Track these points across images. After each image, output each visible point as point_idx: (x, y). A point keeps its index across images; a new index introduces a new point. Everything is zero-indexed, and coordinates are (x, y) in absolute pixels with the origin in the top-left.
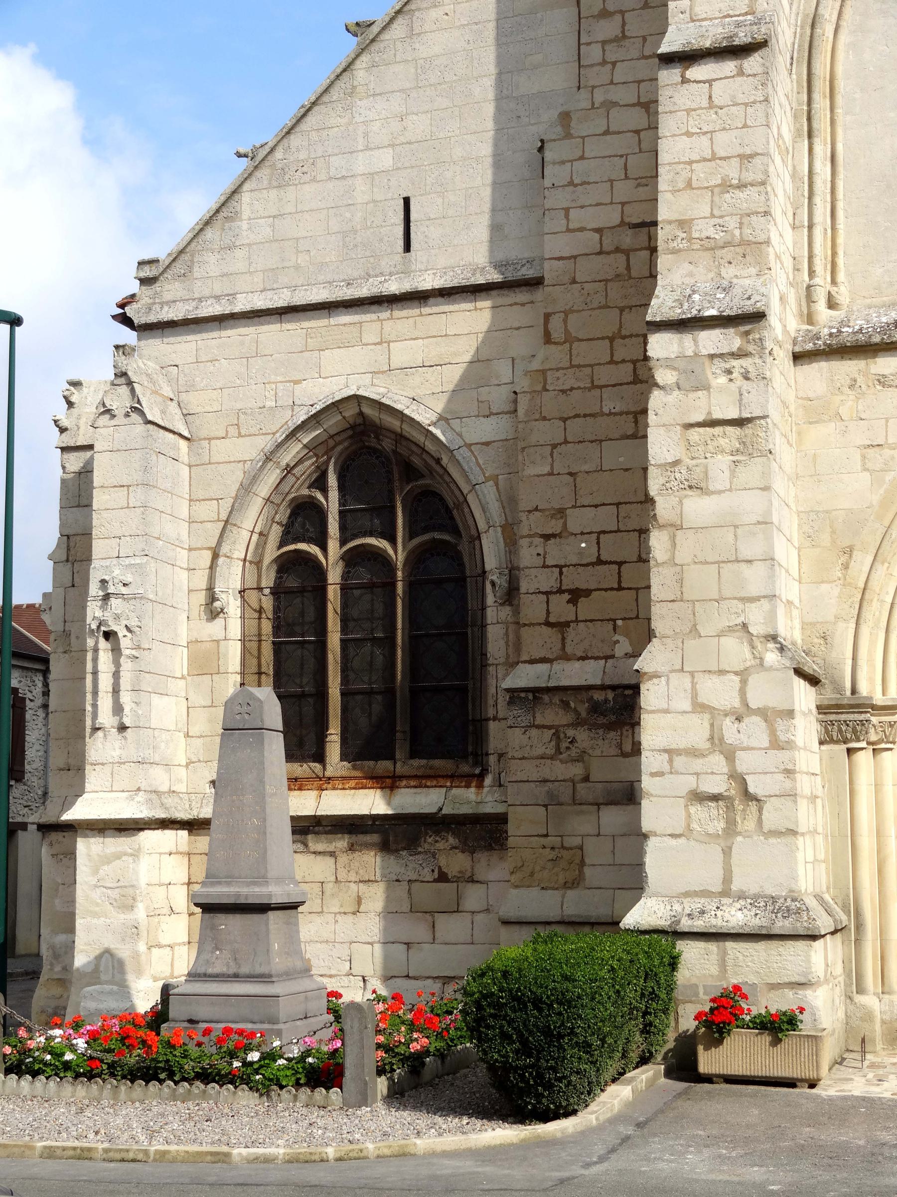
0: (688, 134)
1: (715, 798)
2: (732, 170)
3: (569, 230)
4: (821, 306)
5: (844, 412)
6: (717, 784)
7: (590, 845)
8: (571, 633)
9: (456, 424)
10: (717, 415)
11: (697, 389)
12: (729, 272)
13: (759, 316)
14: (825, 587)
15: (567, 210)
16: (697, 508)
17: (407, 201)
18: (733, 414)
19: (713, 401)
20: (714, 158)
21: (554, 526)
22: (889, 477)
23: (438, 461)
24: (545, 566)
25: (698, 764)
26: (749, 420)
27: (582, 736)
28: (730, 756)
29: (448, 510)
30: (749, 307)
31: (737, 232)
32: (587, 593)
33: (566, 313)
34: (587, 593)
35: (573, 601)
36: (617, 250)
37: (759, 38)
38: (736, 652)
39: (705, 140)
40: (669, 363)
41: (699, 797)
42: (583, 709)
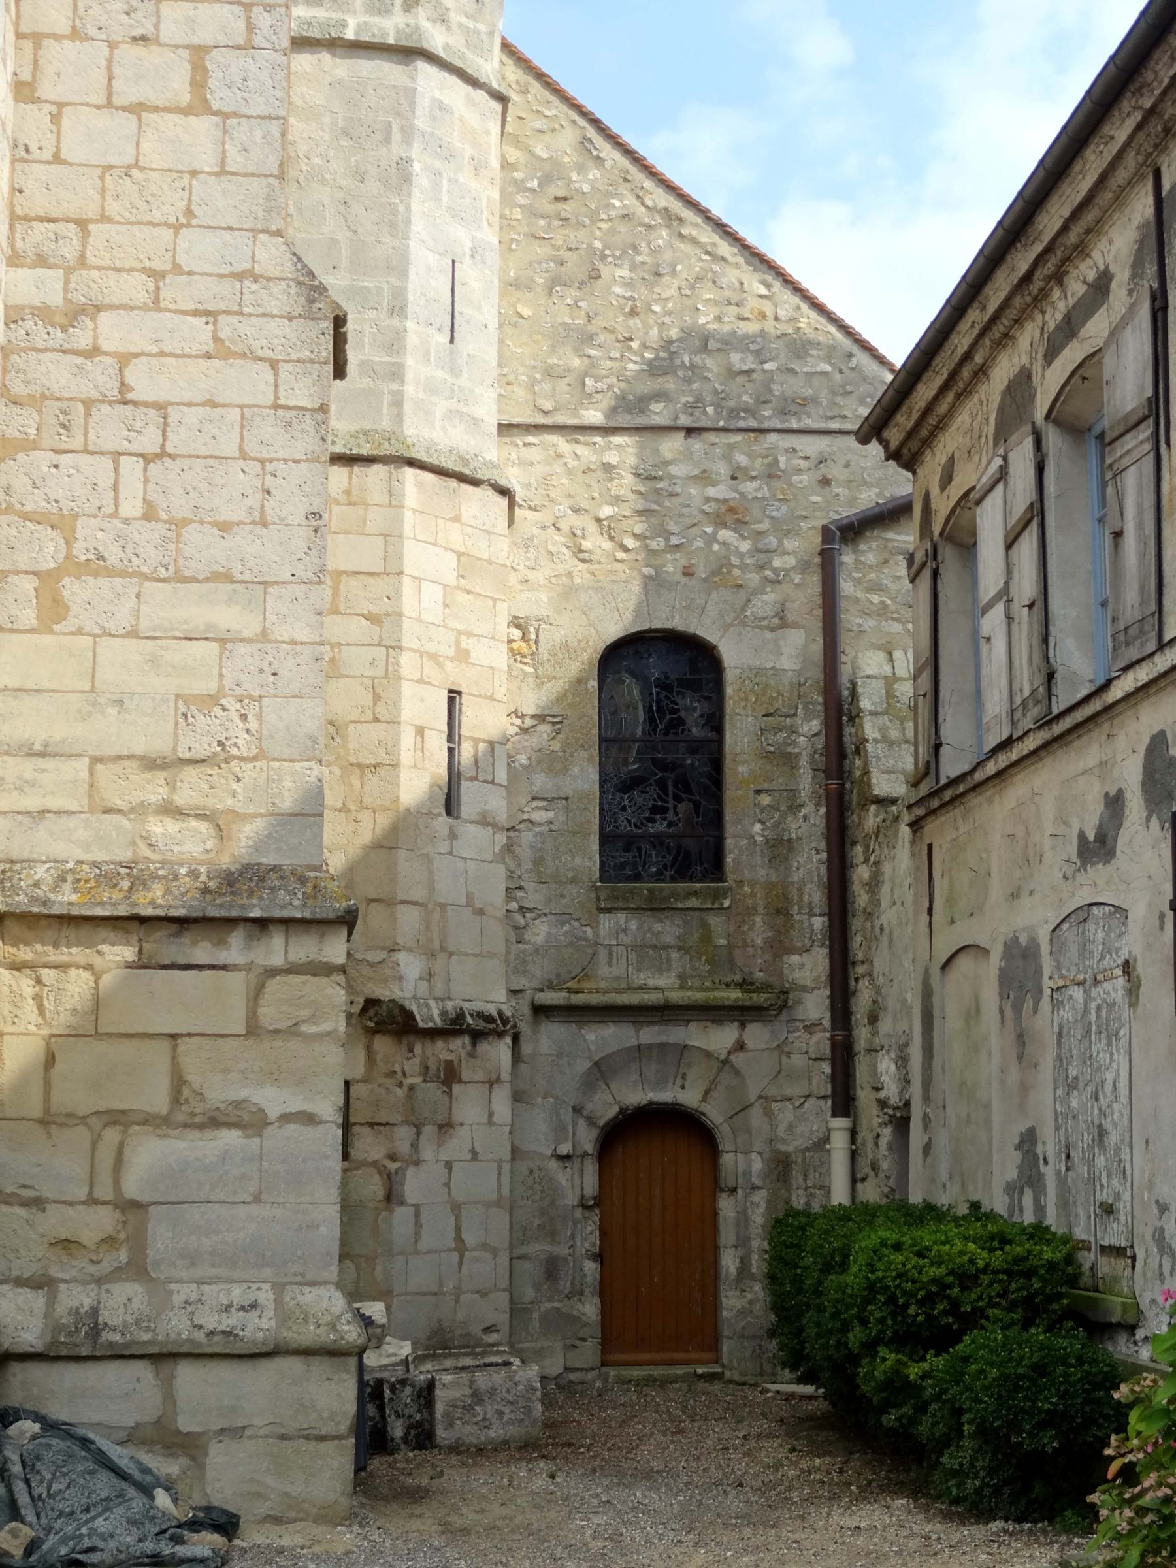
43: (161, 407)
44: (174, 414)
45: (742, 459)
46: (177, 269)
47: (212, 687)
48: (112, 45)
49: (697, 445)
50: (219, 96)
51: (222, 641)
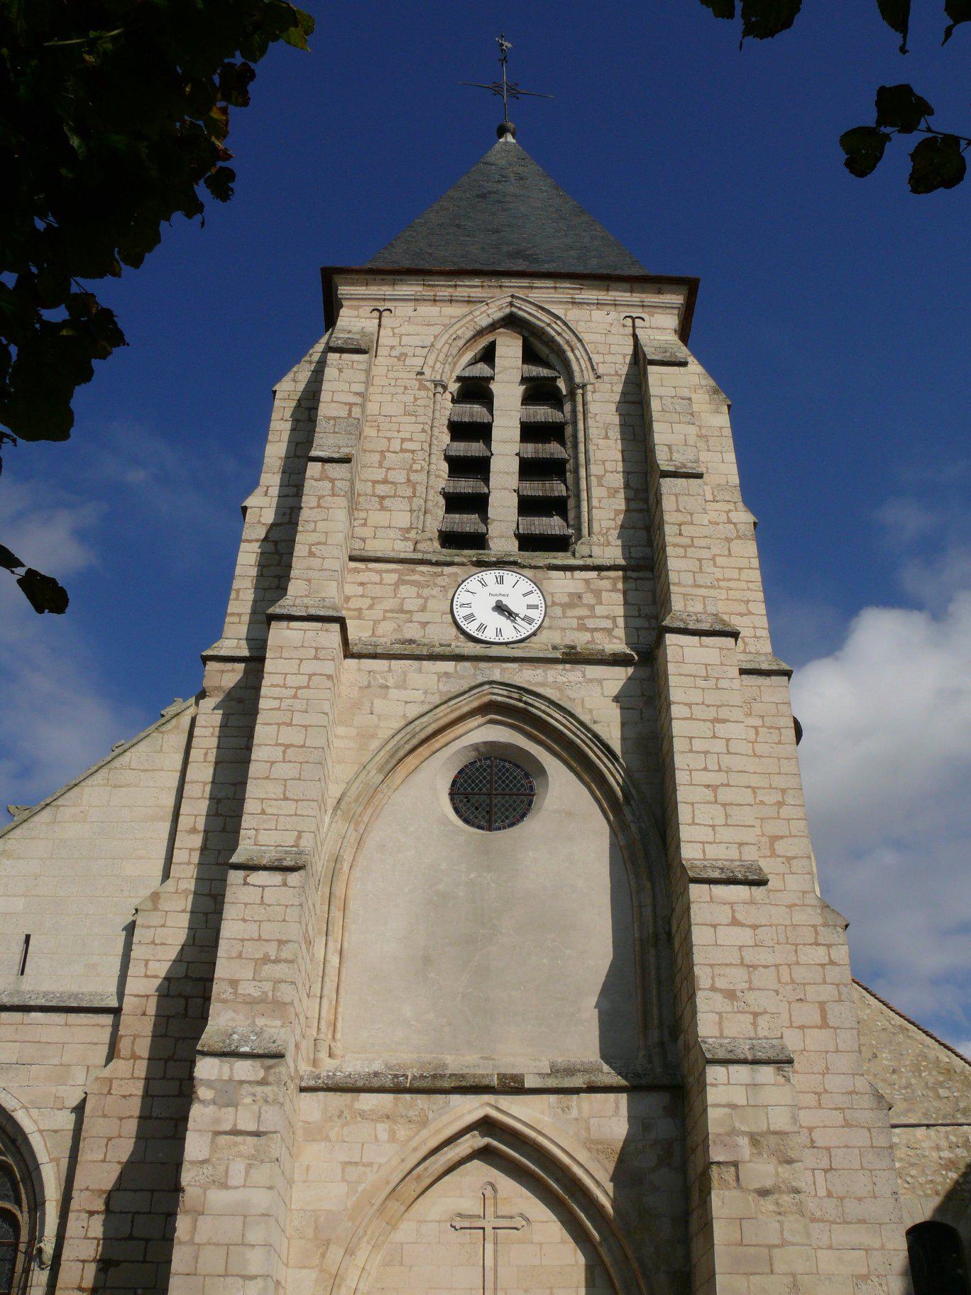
0: (244, 920)
2: (272, 950)
3: (147, 976)
4: (323, 1055)
5: (333, 1134)
9: (34, 1112)
10: (241, 1127)
11: (228, 1105)
12: (260, 1022)
13: (280, 1056)
14: (305, 1271)
15: (147, 961)
16: (217, 1198)
17: (28, 937)
19: (239, 1115)
20: (260, 939)
22: (360, 1189)
24: (86, 1238)
26: (264, 1133)
30: (273, 1048)
31: (270, 994)
32: (117, 1263)
33: (135, 1037)
34: (117, 1263)
36: (180, 995)
37: (300, 863)
39: (255, 927)
40: (209, 1084)
43: (828, 1149)
44: (833, 1152)
45: (953, 1139)
46: (826, 1091)
47: (864, 1271)
48: (789, 1003)
49: (932, 1131)
50: (832, 1021)
51: (866, 1250)
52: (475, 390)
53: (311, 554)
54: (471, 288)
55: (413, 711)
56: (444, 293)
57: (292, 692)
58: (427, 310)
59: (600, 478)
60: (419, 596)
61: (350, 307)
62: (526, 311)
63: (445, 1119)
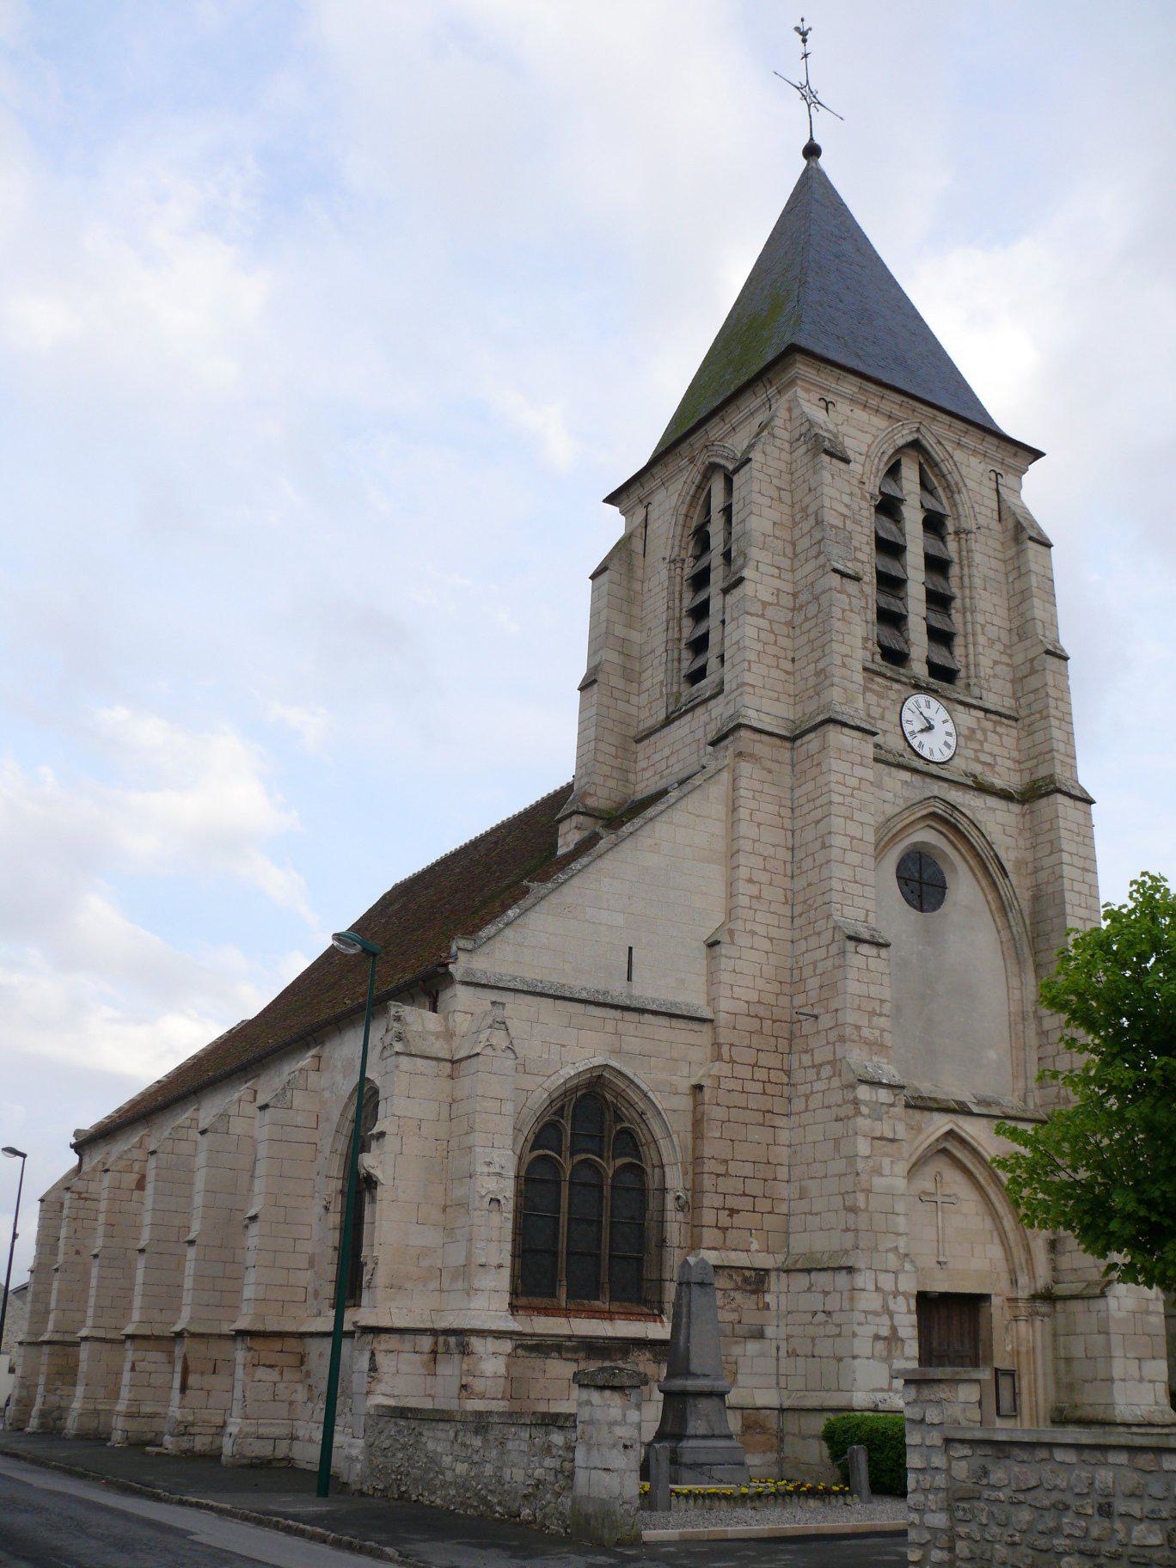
1: (885, 1338)
2: (876, 1005)
6: (885, 1332)
7: (741, 1360)
8: (730, 1233)
18: (891, 1136)
21: (721, 1169)
23: (641, 1114)
25: (878, 1320)
27: (738, 1295)
28: (892, 1318)
29: (636, 1146)
32: (738, 1211)
34: (738, 1211)
35: (730, 1215)
38: (892, 1261)
39: (864, 986)
41: (877, 1337)
42: (739, 1279)
52: (888, 507)
53: (844, 665)
54: (892, 403)
55: (890, 810)
56: (873, 402)
57: (848, 791)
58: (861, 415)
59: (983, 626)
60: (879, 705)
61: (807, 391)
62: (929, 442)
63: (931, 1129)
